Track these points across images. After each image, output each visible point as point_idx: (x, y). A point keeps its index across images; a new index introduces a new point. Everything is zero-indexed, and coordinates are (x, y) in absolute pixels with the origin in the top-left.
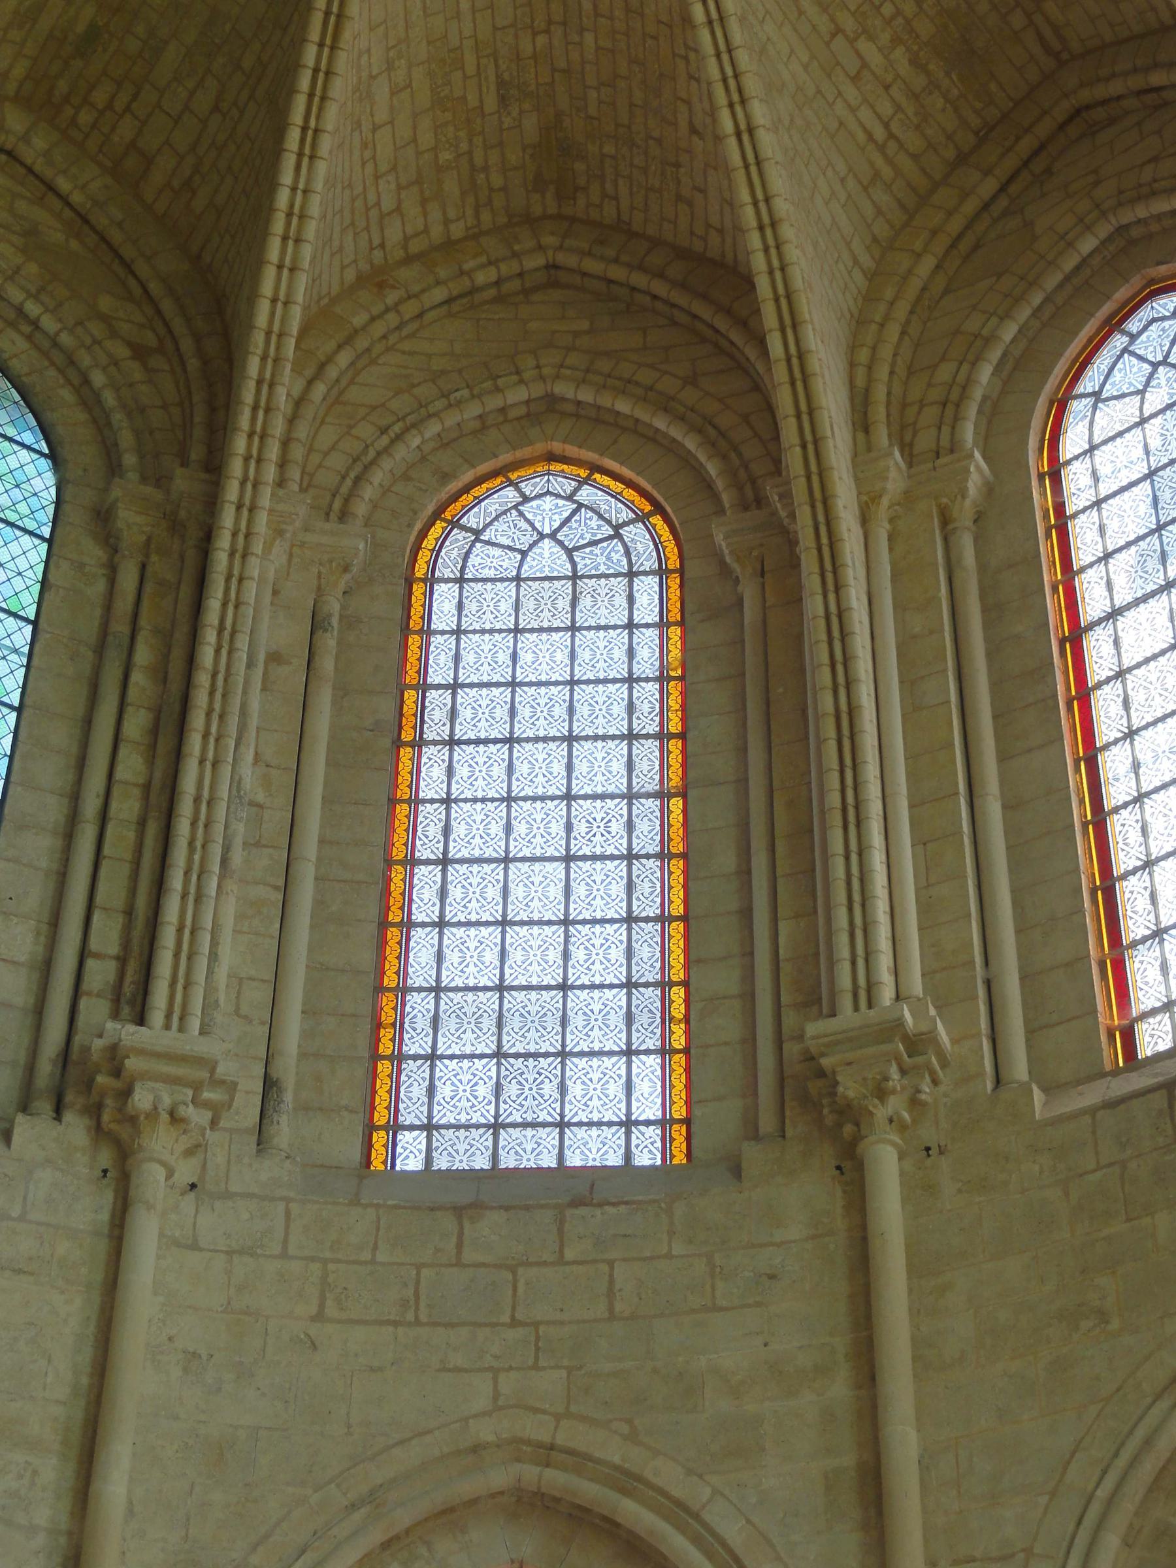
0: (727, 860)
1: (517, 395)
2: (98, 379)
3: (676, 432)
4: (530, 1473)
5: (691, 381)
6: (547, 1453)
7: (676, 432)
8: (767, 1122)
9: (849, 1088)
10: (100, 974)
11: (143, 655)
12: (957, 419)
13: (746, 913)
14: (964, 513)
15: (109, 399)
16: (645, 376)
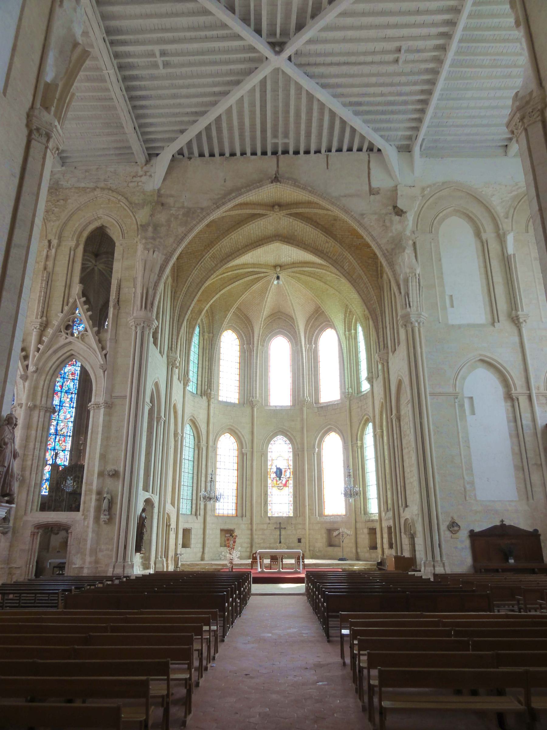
0: (243, 378)
1: (230, 325)
2: (204, 320)
3: (242, 333)
4: (231, 427)
5: (243, 328)
6: (232, 426)
7: (242, 333)
8: (246, 402)
9: (254, 404)
10: (206, 383)
11: (207, 352)
12: (264, 342)
13: (244, 382)
14: (264, 352)
15: (204, 322)
16: (240, 326)
